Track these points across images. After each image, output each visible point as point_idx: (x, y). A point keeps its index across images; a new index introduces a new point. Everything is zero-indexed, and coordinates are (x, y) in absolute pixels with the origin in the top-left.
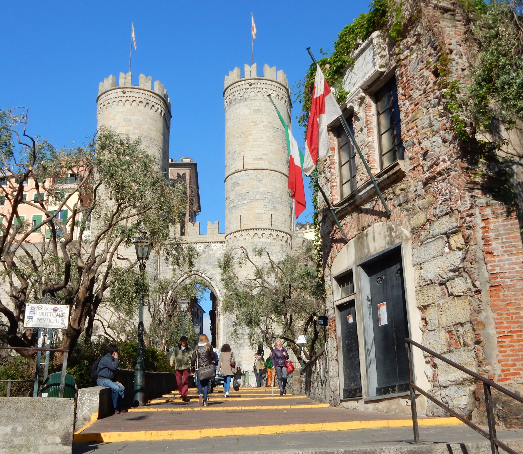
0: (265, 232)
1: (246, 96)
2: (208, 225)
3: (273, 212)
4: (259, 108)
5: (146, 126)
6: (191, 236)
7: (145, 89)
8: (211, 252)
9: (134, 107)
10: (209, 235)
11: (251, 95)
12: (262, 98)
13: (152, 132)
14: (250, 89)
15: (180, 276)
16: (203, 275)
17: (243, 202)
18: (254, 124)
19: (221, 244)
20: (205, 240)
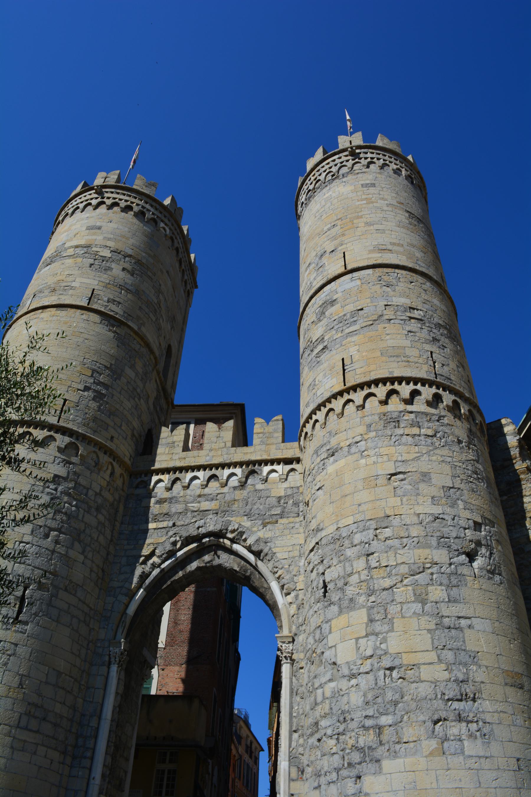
0: (419, 387)
1: (344, 170)
2: (256, 426)
3: (434, 349)
4: (373, 182)
6: (211, 450)
8: (260, 486)
10: (258, 447)
11: (354, 168)
12: (378, 171)
14: (351, 161)
15: (169, 547)
16: (236, 547)
17: (347, 331)
18: (365, 202)
20: (246, 458)
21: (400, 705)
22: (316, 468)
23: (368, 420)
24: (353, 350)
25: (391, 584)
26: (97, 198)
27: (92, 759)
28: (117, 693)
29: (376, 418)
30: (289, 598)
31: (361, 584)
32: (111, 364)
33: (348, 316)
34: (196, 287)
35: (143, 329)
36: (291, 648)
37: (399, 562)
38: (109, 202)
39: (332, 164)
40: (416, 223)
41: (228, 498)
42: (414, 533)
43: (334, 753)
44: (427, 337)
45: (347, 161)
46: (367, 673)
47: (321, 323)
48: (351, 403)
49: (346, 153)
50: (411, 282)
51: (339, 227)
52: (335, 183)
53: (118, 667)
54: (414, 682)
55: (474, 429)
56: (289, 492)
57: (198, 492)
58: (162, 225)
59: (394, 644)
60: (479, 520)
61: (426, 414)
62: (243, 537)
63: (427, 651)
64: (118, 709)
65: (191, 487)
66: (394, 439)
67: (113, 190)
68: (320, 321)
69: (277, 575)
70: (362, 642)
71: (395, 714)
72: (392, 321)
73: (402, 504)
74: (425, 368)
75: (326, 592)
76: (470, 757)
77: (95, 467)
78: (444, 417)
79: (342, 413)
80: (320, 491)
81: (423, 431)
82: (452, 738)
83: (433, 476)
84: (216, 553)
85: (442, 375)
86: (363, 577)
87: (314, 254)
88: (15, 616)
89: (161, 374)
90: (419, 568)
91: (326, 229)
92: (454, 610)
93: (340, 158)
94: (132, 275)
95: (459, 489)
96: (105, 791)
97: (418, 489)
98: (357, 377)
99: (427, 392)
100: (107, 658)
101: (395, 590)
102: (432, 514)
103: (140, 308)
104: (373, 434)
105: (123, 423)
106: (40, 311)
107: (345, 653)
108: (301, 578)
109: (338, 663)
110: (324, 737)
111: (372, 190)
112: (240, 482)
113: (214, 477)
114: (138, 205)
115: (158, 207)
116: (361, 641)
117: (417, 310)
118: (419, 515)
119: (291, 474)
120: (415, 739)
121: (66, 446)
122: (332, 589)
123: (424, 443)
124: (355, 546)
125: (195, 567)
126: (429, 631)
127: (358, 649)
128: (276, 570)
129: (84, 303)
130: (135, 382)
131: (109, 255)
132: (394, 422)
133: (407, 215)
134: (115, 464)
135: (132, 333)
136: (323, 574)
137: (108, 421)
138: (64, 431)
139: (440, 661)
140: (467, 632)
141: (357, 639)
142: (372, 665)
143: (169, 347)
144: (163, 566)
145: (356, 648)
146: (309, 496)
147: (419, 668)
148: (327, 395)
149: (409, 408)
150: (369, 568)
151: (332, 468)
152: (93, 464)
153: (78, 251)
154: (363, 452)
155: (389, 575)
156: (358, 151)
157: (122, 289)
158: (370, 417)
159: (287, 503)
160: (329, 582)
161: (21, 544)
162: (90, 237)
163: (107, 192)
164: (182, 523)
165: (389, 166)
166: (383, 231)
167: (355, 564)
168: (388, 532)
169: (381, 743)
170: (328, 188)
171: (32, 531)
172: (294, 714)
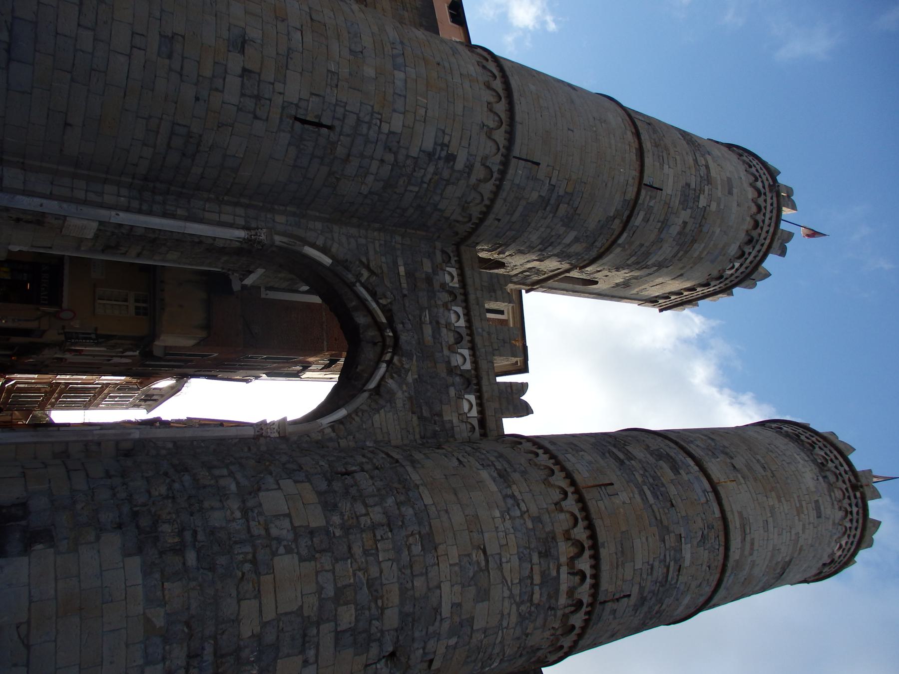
0: (589, 581)
1: (832, 478)
3: (633, 600)
4: (823, 515)
5: (718, 230)
6: (489, 334)
7: (777, 237)
8: (452, 392)
9: (749, 208)
11: (836, 490)
12: (837, 521)
13: (703, 245)
16: (384, 366)
17: (645, 488)
18: (798, 505)
19: (475, 423)
21: (210, 574)
22: (483, 457)
23: (546, 518)
24: (624, 496)
25: (357, 557)
26: (764, 187)
27: (140, 212)
28: (214, 239)
29: (548, 528)
30: (329, 430)
31: (355, 520)
32: (579, 215)
33: (663, 489)
34: (661, 311)
35: (618, 250)
36: (272, 436)
37: (383, 565)
38: (761, 201)
39: (837, 462)
40: (778, 571)
41: (438, 355)
42: (419, 583)
43: (149, 492)
44: (647, 590)
45: (844, 482)
46: (249, 531)
47: (648, 456)
48: (562, 496)
49: (852, 478)
50: (709, 567)
51: (764, 474)
52: (813, 466)
53: (244, 239)
54: (238, 593)
55: (540, 653)
56: (448, 426)
57: (443, 321)
58: (737, 265)
59: (285, 563)
60: (435, 665)
61: (557, 591)
62: (395, 375)
63: (277, 608)
64: (197, 240)
65: (446, 313)
66: (526, 552)
67: (775, 205)
68: (651, 455)
69: (354, 416)
70: (286, 523)
71: (198, 569)
72: (662, 545)
73: (450, 565)
74: (611, 589)
75: (343, 474)
76: (143, 672)
77: (466, 202)
78: (555, 616)
79: (551, 485)
80: (457, 463)
81: (537, 588)
82: (167, 647)
83: (486, 603)
84: (375, 344)
85: (603, 610)
86: (363, 520)
87: (726, 444)
88: (298, 116)
89: (568, 275)
90: (376, 591)
91: (759, 457)
92: (327, 641)
93: (846, 472)
94: (680, 233)
95: (471, 637)
96: (102, 228)
97: (470, 586)
98: (594, 502)
99: (584, 593)
100: (253, 225)
101: (349, 561)
102: (440, 603)
103: (642, 245)
104: (530, 525)
105: (514, 232)
106: (634, 130)
107: (273, 500)
108: (352, 444)
109: (261, 494)
110: (168, 481)
111: (813, 514)
112: (457, 367)
113: (459, 339)
114: (760, 235)
115: (758, 259)
116: (287, 521)
117: (678, 576)
118: (439, 587)
119: (469, 426)
120: (167, 598)
121: (488, 167)
122: (346, 482)
123: (524, 590)
124: (399, 509)
125: (359, 322)
126: (301, 607)
127: (277, 517)
128: (360, 414)
129: (646, 180)
130: (560, 243)
131: (700, 206)
132: (546, 551)
133: (787, 559)
134: (470, 225)
135: (614, 237)
136: (363, 470)
137: (517, 214)
138: (505, 164)
139: (264, 625)
140: (299, 660)
141: (289, 515)
142: (259, 536)
143: (596, 283)
144: (358, 284)
145: (279, 515)
146: (450, 450)
147: (255, 597)
148: (568, 466)
149: (564, 570)
150: (374, 527)
151: (484, 474)
152: (469, 200)
153: (703, 169)
154: (509, 514)
155: (366, 553)
156: (858, 494)
157: (663, 222)
158: (548, 520)
159: (435, 423)
160: (353, 477)
161: (378, 122)
162: (719, 182)
163: (772, 198)
164: (407, 305)
165: (844, 533)
166: (766, 530)
167: (378, 509)
168: (417, 549)
169: (161, 553)
170: (806, 458)
171: (394, 133)
172: (195, 443)
